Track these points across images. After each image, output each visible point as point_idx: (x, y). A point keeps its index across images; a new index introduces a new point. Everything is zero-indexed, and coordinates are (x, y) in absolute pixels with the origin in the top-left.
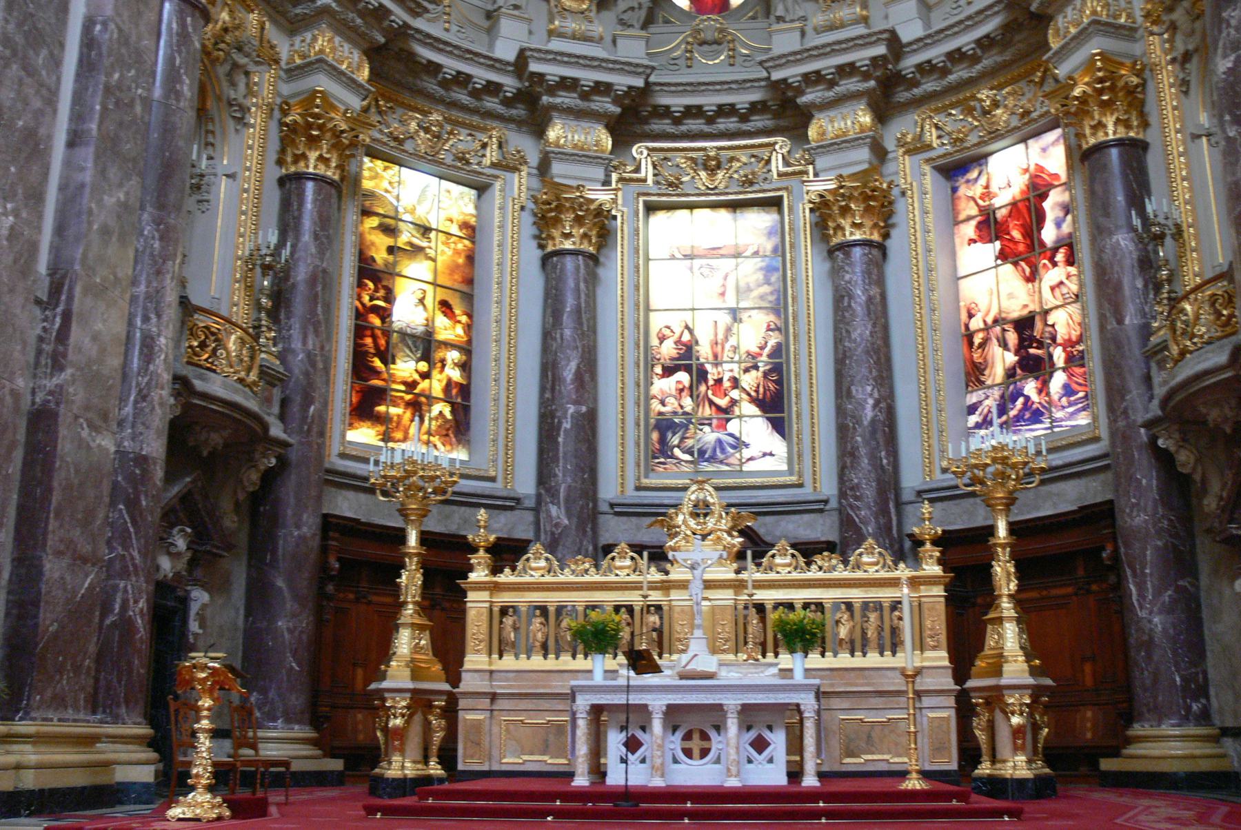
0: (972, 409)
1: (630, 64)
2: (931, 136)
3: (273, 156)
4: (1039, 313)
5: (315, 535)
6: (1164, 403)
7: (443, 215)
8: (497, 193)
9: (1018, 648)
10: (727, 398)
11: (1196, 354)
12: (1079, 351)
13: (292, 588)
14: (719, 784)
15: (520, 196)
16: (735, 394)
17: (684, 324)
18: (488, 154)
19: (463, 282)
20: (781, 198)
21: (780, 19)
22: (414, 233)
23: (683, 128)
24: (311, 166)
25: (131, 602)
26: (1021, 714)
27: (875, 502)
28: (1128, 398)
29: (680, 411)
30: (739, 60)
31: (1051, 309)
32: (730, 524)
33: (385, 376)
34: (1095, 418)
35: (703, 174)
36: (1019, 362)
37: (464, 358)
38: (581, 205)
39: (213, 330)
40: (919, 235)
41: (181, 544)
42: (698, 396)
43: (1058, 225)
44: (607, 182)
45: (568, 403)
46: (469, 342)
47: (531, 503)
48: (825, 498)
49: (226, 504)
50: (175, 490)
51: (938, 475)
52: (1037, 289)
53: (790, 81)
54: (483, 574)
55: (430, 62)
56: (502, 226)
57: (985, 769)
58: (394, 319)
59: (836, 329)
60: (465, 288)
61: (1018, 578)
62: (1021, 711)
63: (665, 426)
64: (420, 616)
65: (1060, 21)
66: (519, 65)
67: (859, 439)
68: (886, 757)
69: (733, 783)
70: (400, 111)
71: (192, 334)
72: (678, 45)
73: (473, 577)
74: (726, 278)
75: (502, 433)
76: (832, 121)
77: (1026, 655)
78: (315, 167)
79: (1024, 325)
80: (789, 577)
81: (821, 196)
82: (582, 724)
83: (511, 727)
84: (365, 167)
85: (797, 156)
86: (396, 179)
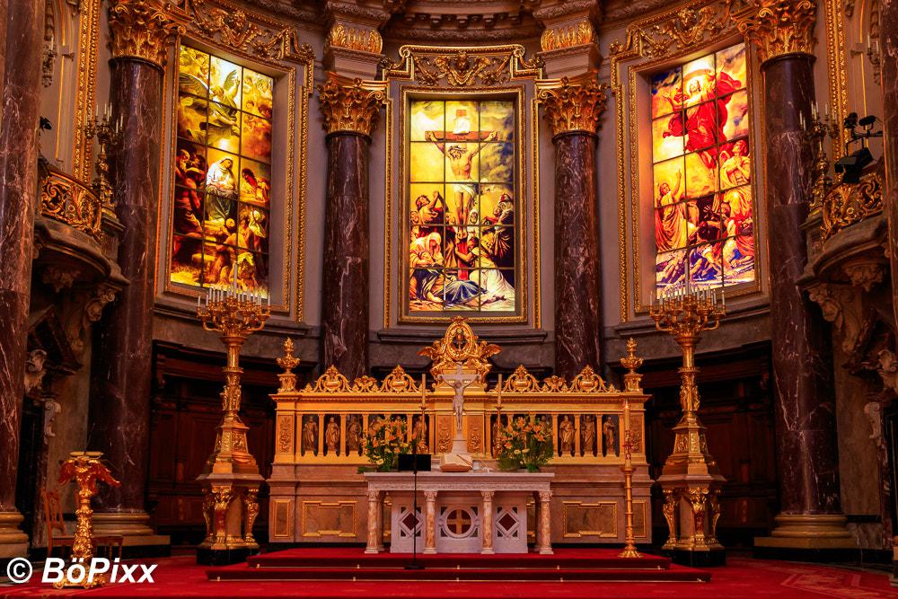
0: (660, 268)
2: (639, 47)
3: (103, 42)
4: (717, 193)
5: (147, 357)
6: (817, 268)
11: (847, 229)
13: (129, 400)
14: (476, 552)
15: (308, 85)
16: (476, 251)
17: (437, 195)
18: (283, 50)
19: (262, 155)
20: (517, 93)
22: (223, 112)
23: (440, 33)
24: (138, 51)
25: (5, 411)
26: (701, 502)
27: (584, 337)
28: (787, 261)
29: (433, 264)
31: (727, 190)
33: (201, 230)
34: (758, 276)
35: (455, 72)
36: (700, 231)
37: (263, 216)
38: (358, 95)
39: (64, 187)
41: (38, 363)
42: (447, 252)
43: (737, 123)
44: (378, 77)
45: (347, 255)
47: (315, 334)
49: (73, 332)
50: (34, 320)
52: (716, 174)
57: (672, 543)
58: (208, 183)
60: (263, 160)
62: (701, 499)
63: (422, 274)
67: (573, 288)
68: (597, 533)
69: (488, 551)
71: (46, 191)
73: (281, 391)
74: (470, 158)
77: (706, 458)
78: (141, 53)
79: (704, 201)
80: (526, 394)
84: (181, 54)
85: (530, 60)
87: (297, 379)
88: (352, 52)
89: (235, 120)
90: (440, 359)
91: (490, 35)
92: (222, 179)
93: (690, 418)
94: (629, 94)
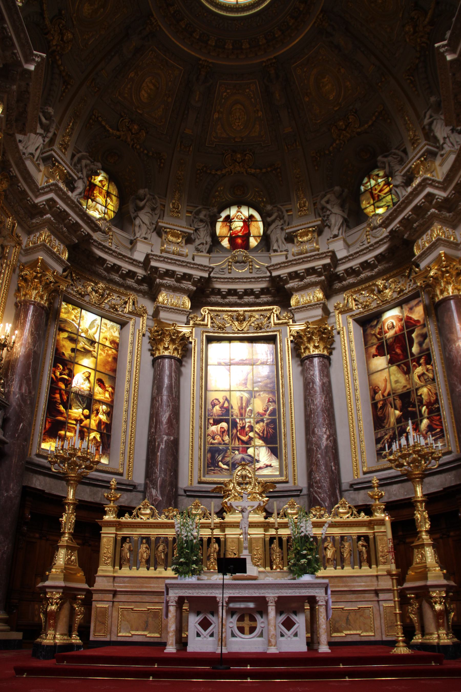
1: (202, 265)
2: (352, 304)
7: (102, 335)
8: (131, 327)
9: (434, 562)
10: (247, 436)
12: (436, 408)
14: (260, 650)
16: (251, 434)
17: (225, 398)
18: (127, 307)
19: (110, 370)
20: (276, 335)
21: (275, 251)
22: (86, 343)
23: (227, 300)
26: (440, 604)
27: (329, 489)
29: (223, 443)
30: (255, 270)
32: (261, 490)
33: (65, 415)
35: (236, 323)
37: (109, 409)
40: (347, 353)
43: (420, 344)
44: (188, 323)
46: (112, 401)
47: (141, 488)
48: (300, 488)
51: (361, 476)
53: (282, 276)
54: (112, 517)
55: (100, 257)
56: (133, 343)
57: (418, 639)
58: (73, 386)
59: (306, 399)
60: (111, 374)
61: (430, 521)
62: (440, 601)
64: (72, 541)
65: (420, 242)
66: (146, 263)
67: (319, 456)
69: (273, 650)
70: (83, 281)
72: (225, 262)
73: (106, 518)
75: (128, 450)
76: (302, 296)
81: (297, 333)
82: (172, 609)
83: (125, 612)
84: (62, 307)
85: (284, 315)
86: (79, 315)
87: (119, 510)
88: (171, 308)
89: (94, 348)
90: (229, 494)
91: (258, 301)
92: (83, 384)
93: (425, 536)
94: (349, 332)
